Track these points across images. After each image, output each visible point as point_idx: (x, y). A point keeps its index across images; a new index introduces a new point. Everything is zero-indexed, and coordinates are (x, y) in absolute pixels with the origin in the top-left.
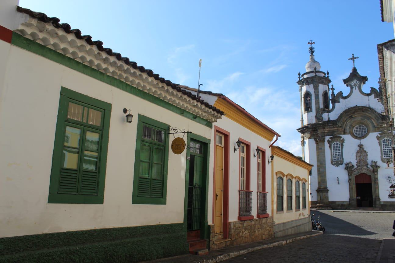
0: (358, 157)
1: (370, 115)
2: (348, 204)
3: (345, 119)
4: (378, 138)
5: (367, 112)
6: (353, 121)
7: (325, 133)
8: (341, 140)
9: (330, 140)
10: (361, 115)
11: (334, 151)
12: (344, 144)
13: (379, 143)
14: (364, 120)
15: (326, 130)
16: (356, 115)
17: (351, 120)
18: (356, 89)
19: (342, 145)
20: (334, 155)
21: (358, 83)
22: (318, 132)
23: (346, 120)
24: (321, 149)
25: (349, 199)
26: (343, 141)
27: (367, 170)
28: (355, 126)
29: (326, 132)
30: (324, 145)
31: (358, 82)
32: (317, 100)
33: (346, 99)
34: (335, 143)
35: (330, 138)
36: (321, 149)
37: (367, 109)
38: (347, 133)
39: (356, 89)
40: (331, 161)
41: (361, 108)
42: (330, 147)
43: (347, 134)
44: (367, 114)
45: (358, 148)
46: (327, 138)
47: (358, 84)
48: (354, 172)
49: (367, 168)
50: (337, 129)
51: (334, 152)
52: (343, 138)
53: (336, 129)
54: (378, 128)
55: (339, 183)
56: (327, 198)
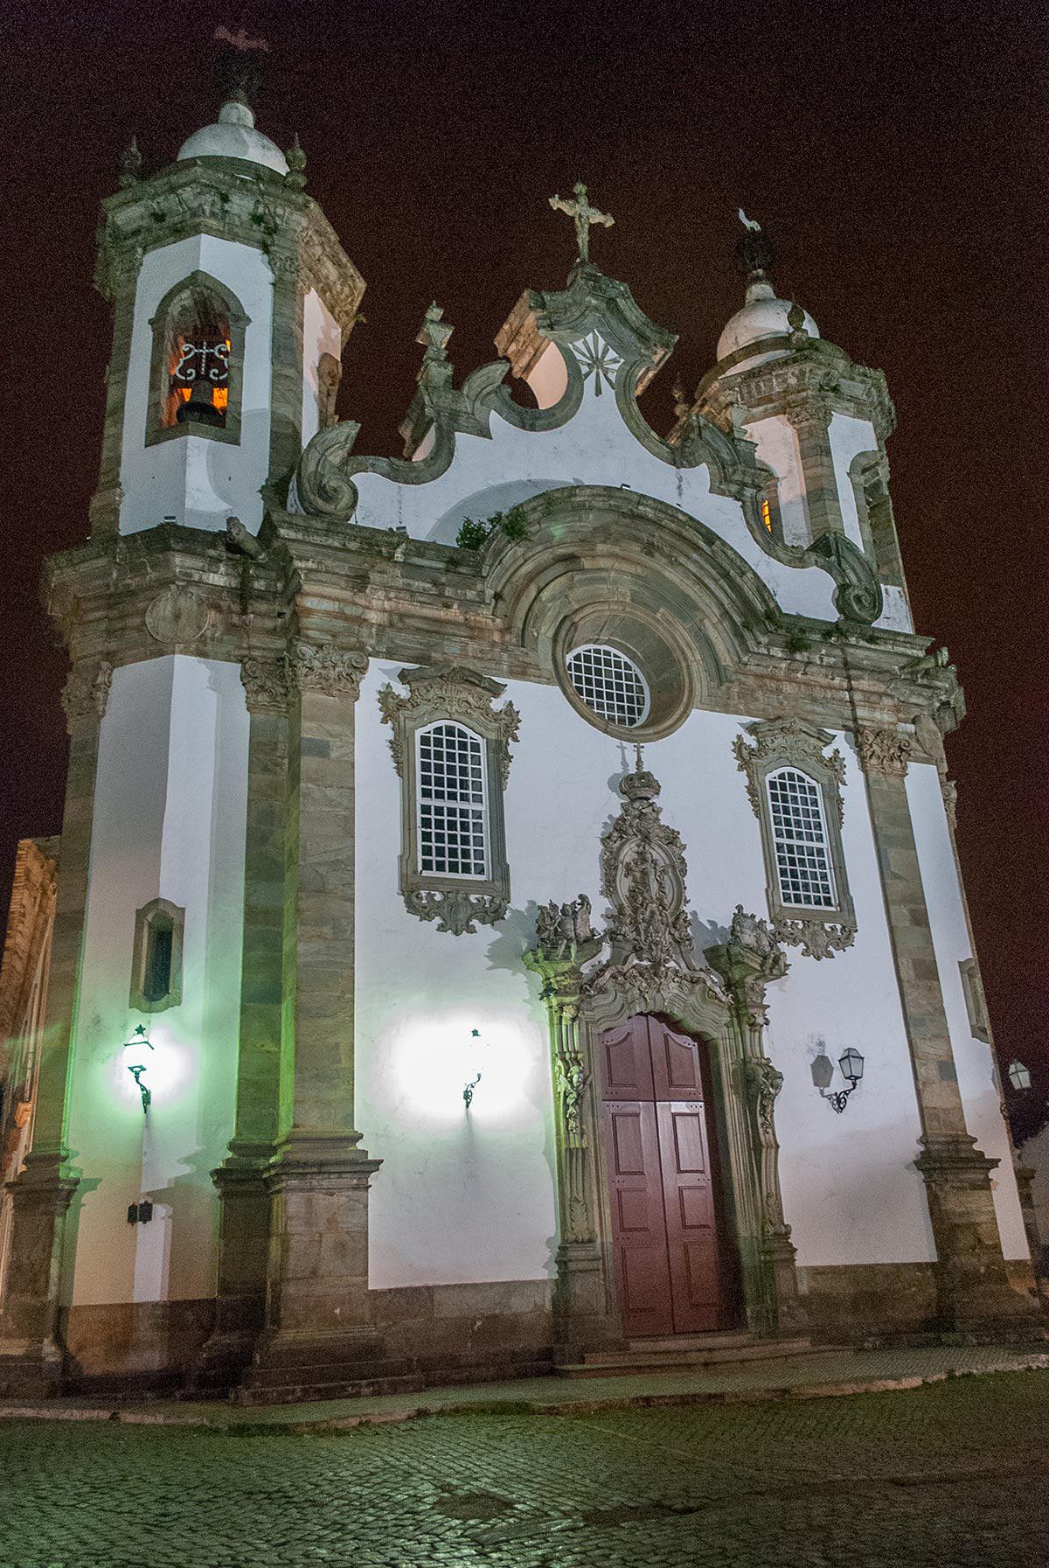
0: (621, 871)
1: (693, 591)
2: (548, 1306)
3: (523, 570)
4: (746, 758)
5: (673, 562)
6: (579, 592)
7: (361, 621)
8: (496, 717)
9: (402, 691)
10: (639, 571)
11: (426, 793)
12: (513, 748)
13: (752, 791)
14: (656, 611)
15: (376, 606)
16: (603, 558)
17: (571, 588)
18: (598, 392)
19: (500, 756)
20: (426, 823)
21: (614, 361)
22: (309, 603)
23: (531, 578)
24: (321, 750)
25: (562, 1262)
26: (510, 721)
27: (691, 992)
28: (577, 646)
29: (374, 617)
30: (348, 720)
31: (612, 354)
32: (291, 372)
33: (533, 428)
34: (438, 730)
35: (403, 676)
36: (321, 750)
37: (689, 533)
38: (537, 667)
39: (598, 392)
40: (403, 877)
41: (650, 514)
42: (398, 747)
43: (539, 679)
44: (672, 575)
45: (615, 805)
46: (379, 674)
47: (616, 366)
48: (602, 991)
49: (686, 971)
50: (461, 619)
51: (434, 802)
52: (510, 704)
53: (455, 613)
54: (747, 694)
55: (467, 1096)
56: (355, 1246)
